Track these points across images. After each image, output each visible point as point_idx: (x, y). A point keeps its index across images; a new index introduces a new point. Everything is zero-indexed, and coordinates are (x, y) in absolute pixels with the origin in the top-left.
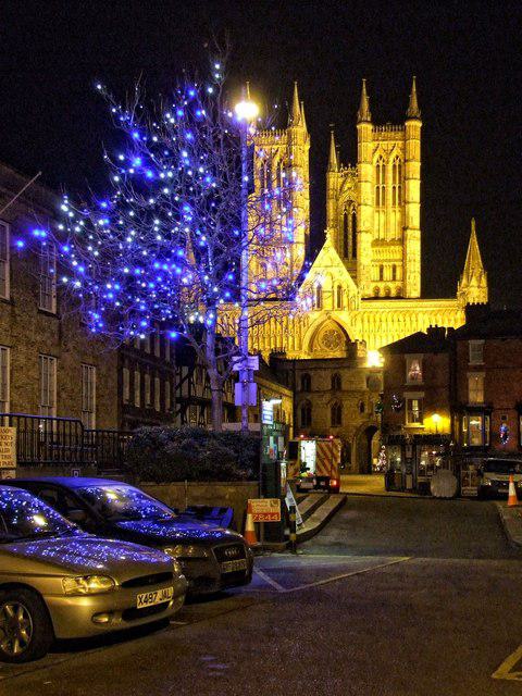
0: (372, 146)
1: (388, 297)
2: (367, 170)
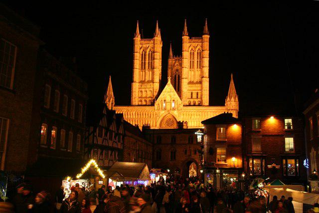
0: (189, 45)
1: (194, 105)
2: (186, 54)
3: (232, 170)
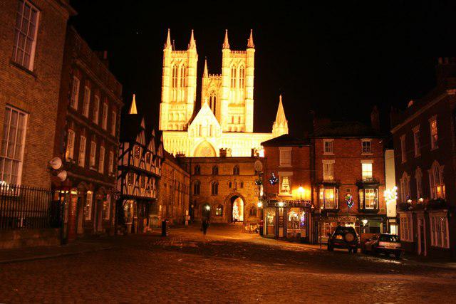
0: (230, 59)
2: (226, 70)
3: (299, 205)
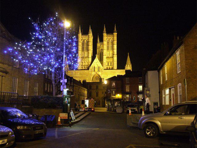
0: (106, 38)
1: (109, 69)
